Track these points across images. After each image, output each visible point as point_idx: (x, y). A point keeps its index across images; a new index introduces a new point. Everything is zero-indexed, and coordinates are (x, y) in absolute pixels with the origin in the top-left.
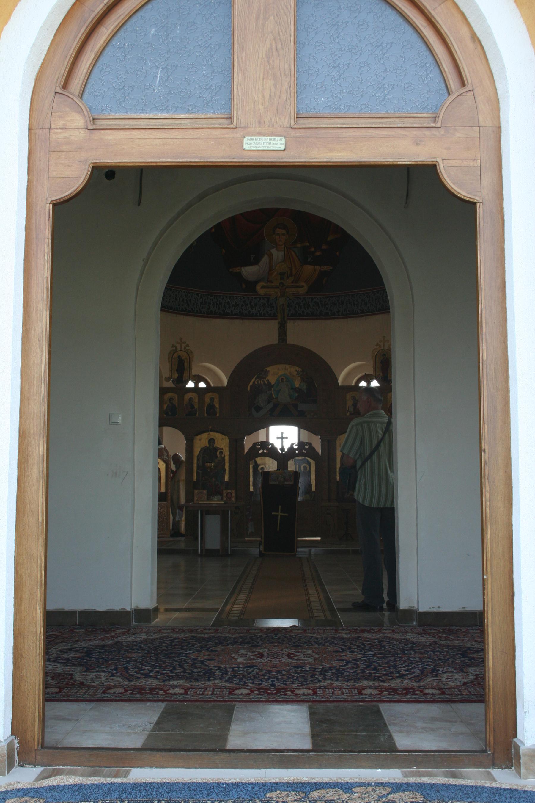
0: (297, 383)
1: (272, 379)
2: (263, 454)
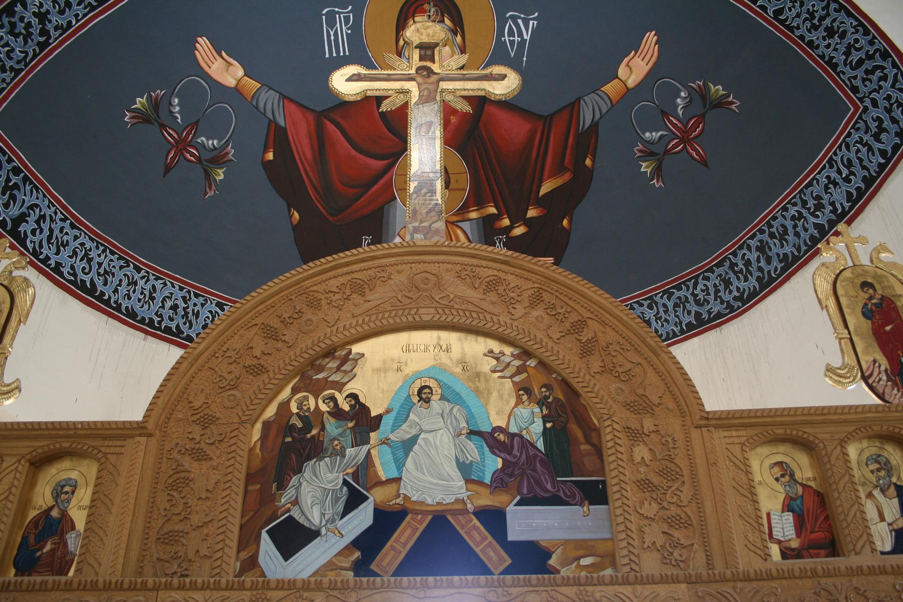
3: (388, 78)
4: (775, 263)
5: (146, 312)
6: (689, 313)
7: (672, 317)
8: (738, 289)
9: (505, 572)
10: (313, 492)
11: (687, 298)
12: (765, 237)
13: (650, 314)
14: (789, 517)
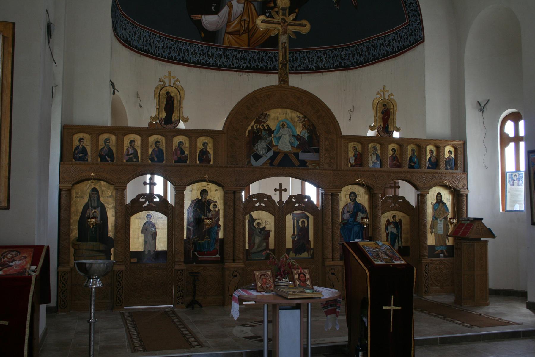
0: (299, 130)
1: (272, 124)
2: (260, 208)
3: (273, 23)
4: (371, 56)
5: (140, 46)
6: (338, 61)
7: (331, 61)
8: (357, 59)
9: (298, 166)
10: (261, 147)
11: (338, 56)
12: (370, 45)
13: (323, 57)
14: (354, 158)
